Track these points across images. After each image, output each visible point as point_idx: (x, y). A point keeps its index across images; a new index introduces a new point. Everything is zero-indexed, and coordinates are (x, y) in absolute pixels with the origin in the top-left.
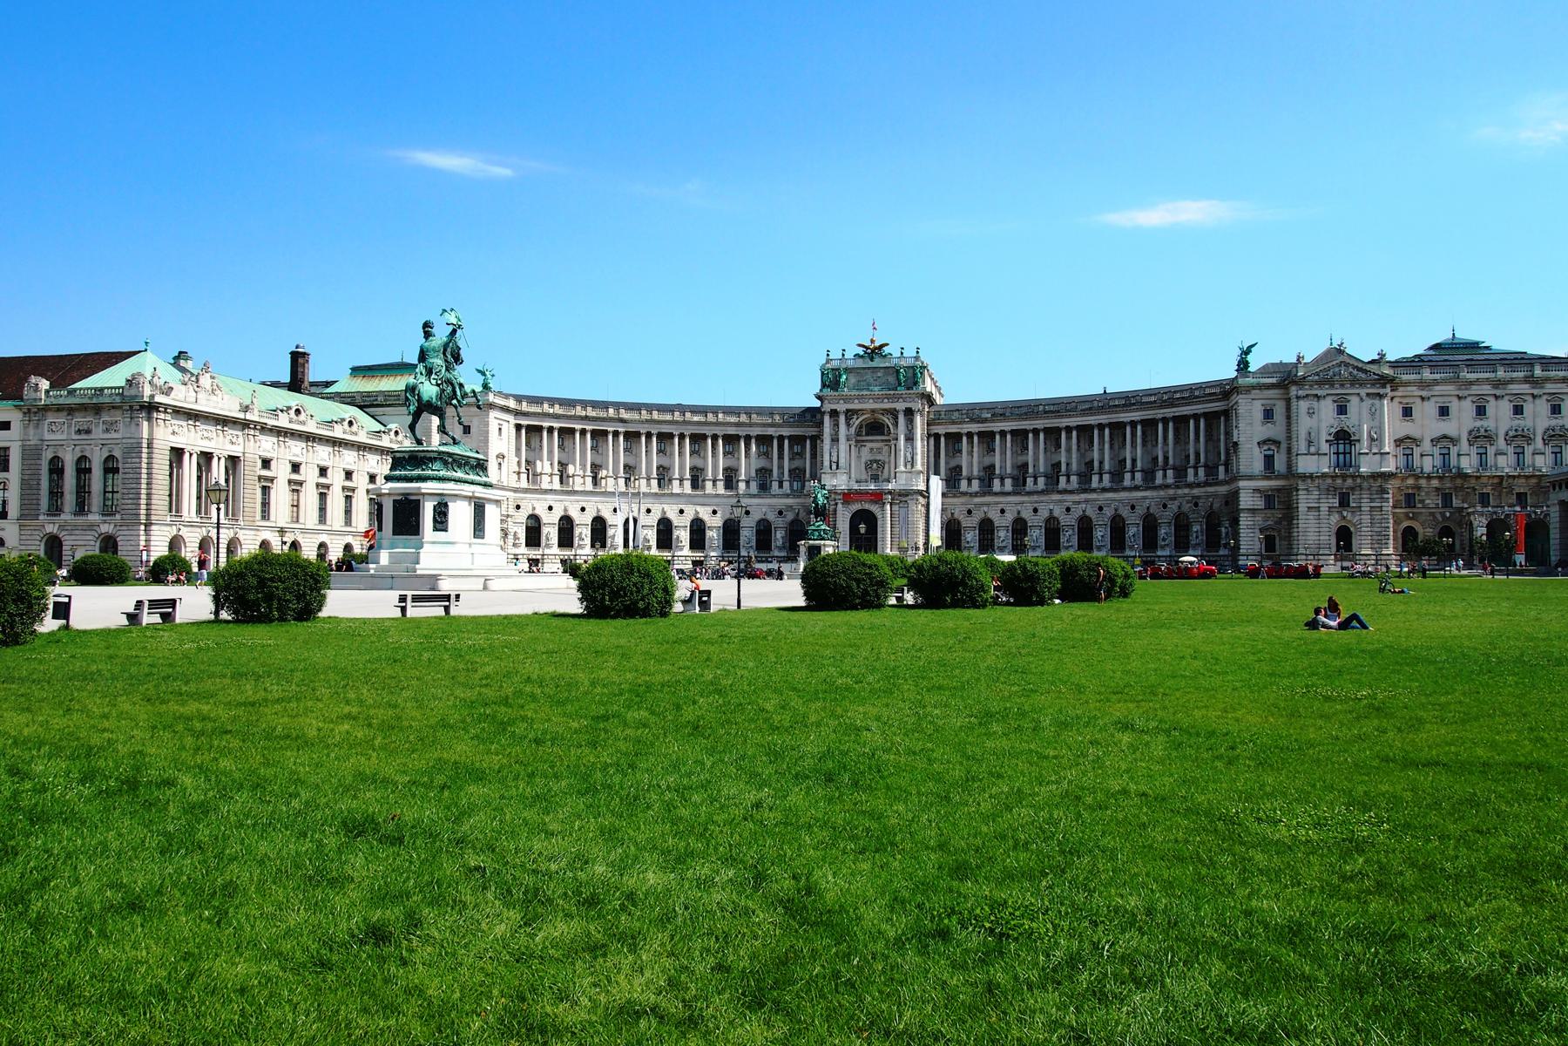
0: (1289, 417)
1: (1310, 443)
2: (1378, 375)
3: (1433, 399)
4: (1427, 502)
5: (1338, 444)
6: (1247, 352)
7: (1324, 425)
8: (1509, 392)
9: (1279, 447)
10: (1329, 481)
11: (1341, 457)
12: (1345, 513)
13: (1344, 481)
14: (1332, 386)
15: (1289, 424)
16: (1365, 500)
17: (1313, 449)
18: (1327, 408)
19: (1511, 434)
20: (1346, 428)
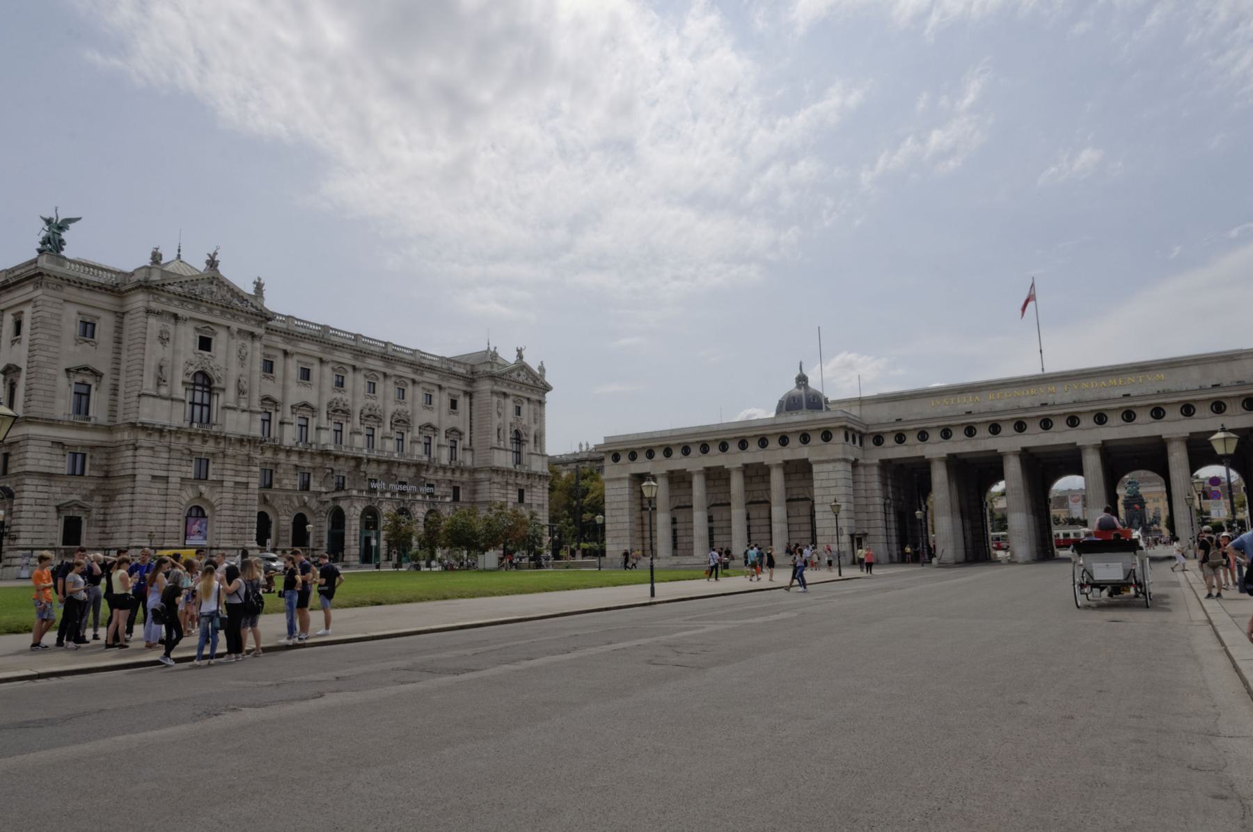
0: (118, 341)
1: (160, 381)
2: (256, 308)
3: (296, 358)
4: (285, 481)
5: (194, 390)
6: (62, 226)
7: (181, 360)
8: (366, 365)
9: (98, 382)
10: (184, 440)
11: (197, 409)
12: (203, 488)
13: (205, 442)
14: (197, 307)
15: (118, 352)
16: (229, 472)
17: (164, 391)
18: (187, 337)
19: (366, 412)
20: (208, 371)
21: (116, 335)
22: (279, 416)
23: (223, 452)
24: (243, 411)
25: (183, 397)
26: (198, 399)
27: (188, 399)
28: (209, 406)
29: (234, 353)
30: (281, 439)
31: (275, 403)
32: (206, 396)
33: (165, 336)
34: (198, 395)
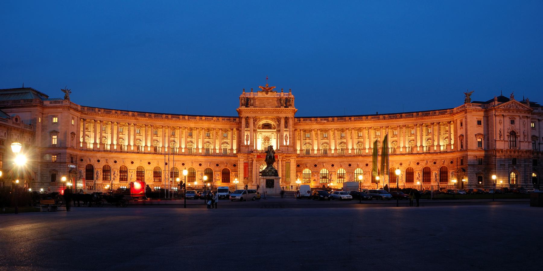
5: (510, 137)
7: (506, 128)
11: (512, 142)
18: (507, 121)
20: (514, 130)
21: (487, 123)
22: (538, 141)
23: (521, 156)
24: (526, 142)
25: (507, 140)
26: (512, 140)
27: (509, 140)
28: (515, 141)
29: (521, 123)
30: (539, 149)
31: (537, 137)
32: (514, 138)
33: (501, 122)
34: (512, 138)
